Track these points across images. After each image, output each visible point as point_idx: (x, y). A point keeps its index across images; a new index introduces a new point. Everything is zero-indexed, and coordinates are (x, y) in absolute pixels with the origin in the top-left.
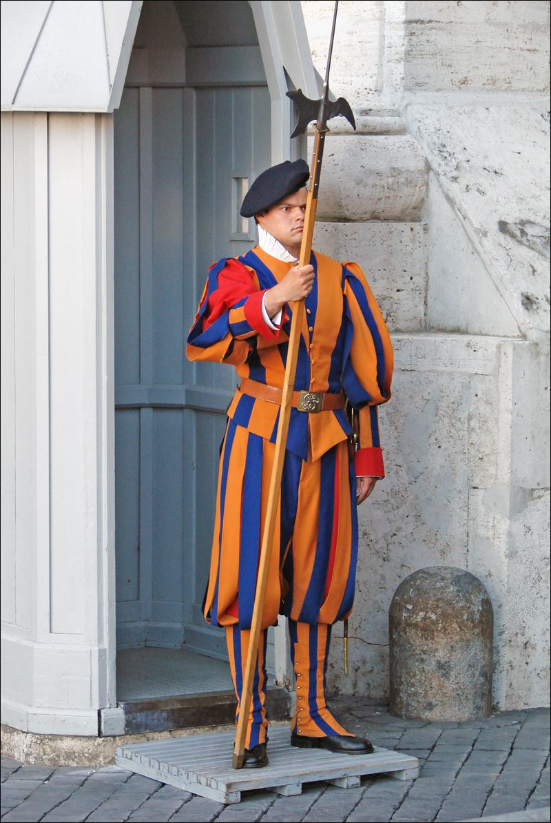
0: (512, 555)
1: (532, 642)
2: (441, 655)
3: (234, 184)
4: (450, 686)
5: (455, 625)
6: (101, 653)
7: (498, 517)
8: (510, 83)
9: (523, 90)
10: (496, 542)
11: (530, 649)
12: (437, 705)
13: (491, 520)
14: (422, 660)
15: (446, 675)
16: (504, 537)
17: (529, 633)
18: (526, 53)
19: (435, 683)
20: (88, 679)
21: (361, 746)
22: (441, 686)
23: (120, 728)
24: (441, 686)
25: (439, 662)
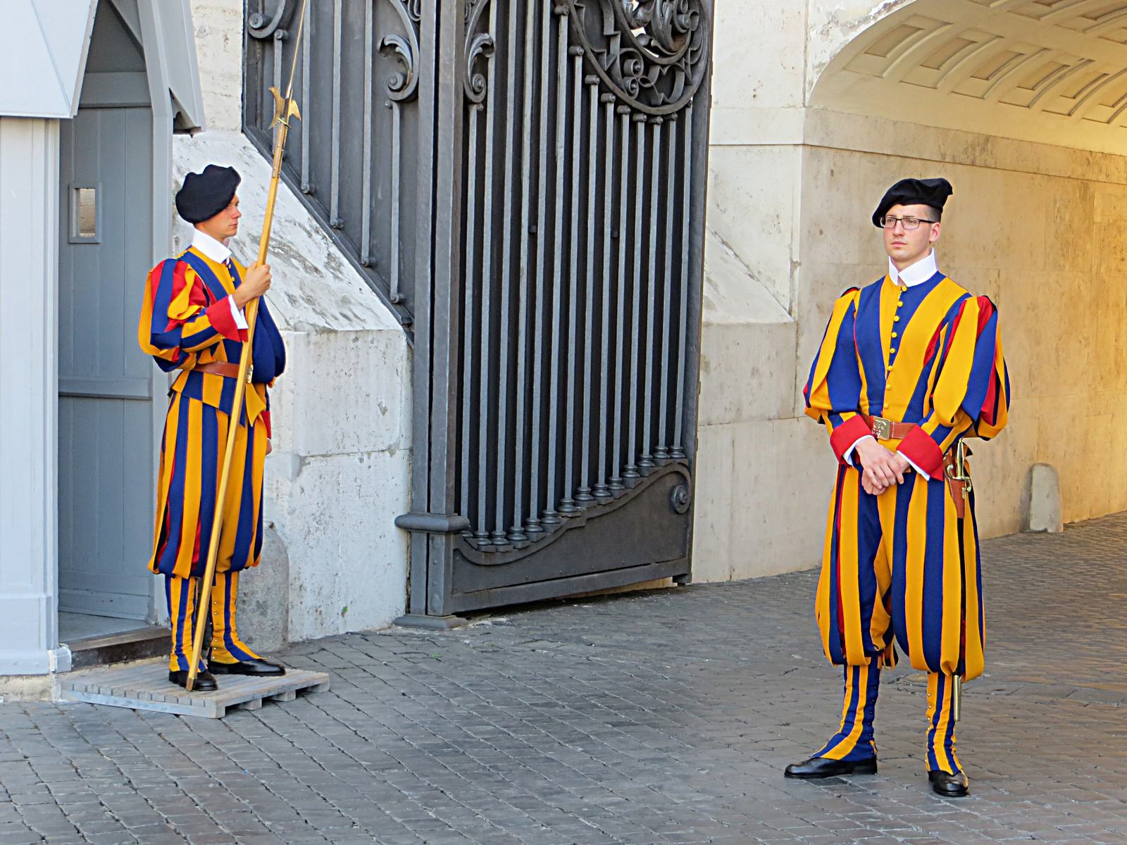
0: (291, 513)
1: (304, 585)
2: (260, 597)
3: (74, 191)
4: (268, 623)
5: (271, 571)
6: (48, 599)
7: (281, 480)
8: (214, 122)
9: (223, 129)
10: (280, 501)
11: (303, 591)
12: (256, 639)
13: (275, 483)
14: (244, 602)
15: (264, 614)
16: (286, 498)
17: (303, 577)
18: (224, 97)
19: (255, 621)
20: (37, 623)
21: (276, 669)
22: (260, 623)
23: (69, 666)
24: (260, 623)
25: (258, 602)
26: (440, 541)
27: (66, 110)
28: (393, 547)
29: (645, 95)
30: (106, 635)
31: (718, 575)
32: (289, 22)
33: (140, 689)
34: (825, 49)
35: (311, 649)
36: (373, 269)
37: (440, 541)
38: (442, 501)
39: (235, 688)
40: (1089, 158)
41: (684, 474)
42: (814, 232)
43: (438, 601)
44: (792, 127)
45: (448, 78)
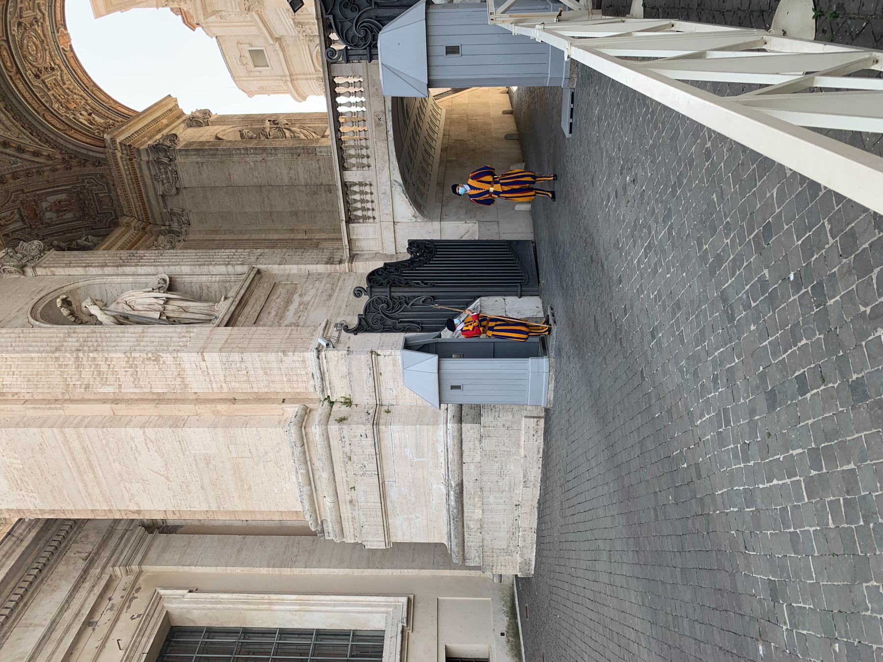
26: (524, 289)
27: (436, 357)
28: (525, 299)
29: (431, 252)
30: (540, 349)
31: (532, 235)
32: (418, 324)
33: (552, 342)
34: (420, 219)
35: (545, 311)
36: (468, 304)
37: (524, 289)
38: (515, 289)
39: (551, 322)
40: (441, 161)
41: (510, 242)
42: (459, 219)
43: (535, 289)
44: (436, 225)
45: (429, 290)
